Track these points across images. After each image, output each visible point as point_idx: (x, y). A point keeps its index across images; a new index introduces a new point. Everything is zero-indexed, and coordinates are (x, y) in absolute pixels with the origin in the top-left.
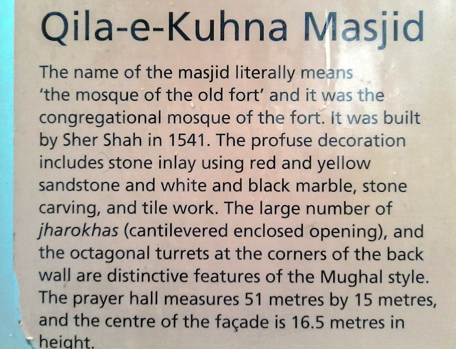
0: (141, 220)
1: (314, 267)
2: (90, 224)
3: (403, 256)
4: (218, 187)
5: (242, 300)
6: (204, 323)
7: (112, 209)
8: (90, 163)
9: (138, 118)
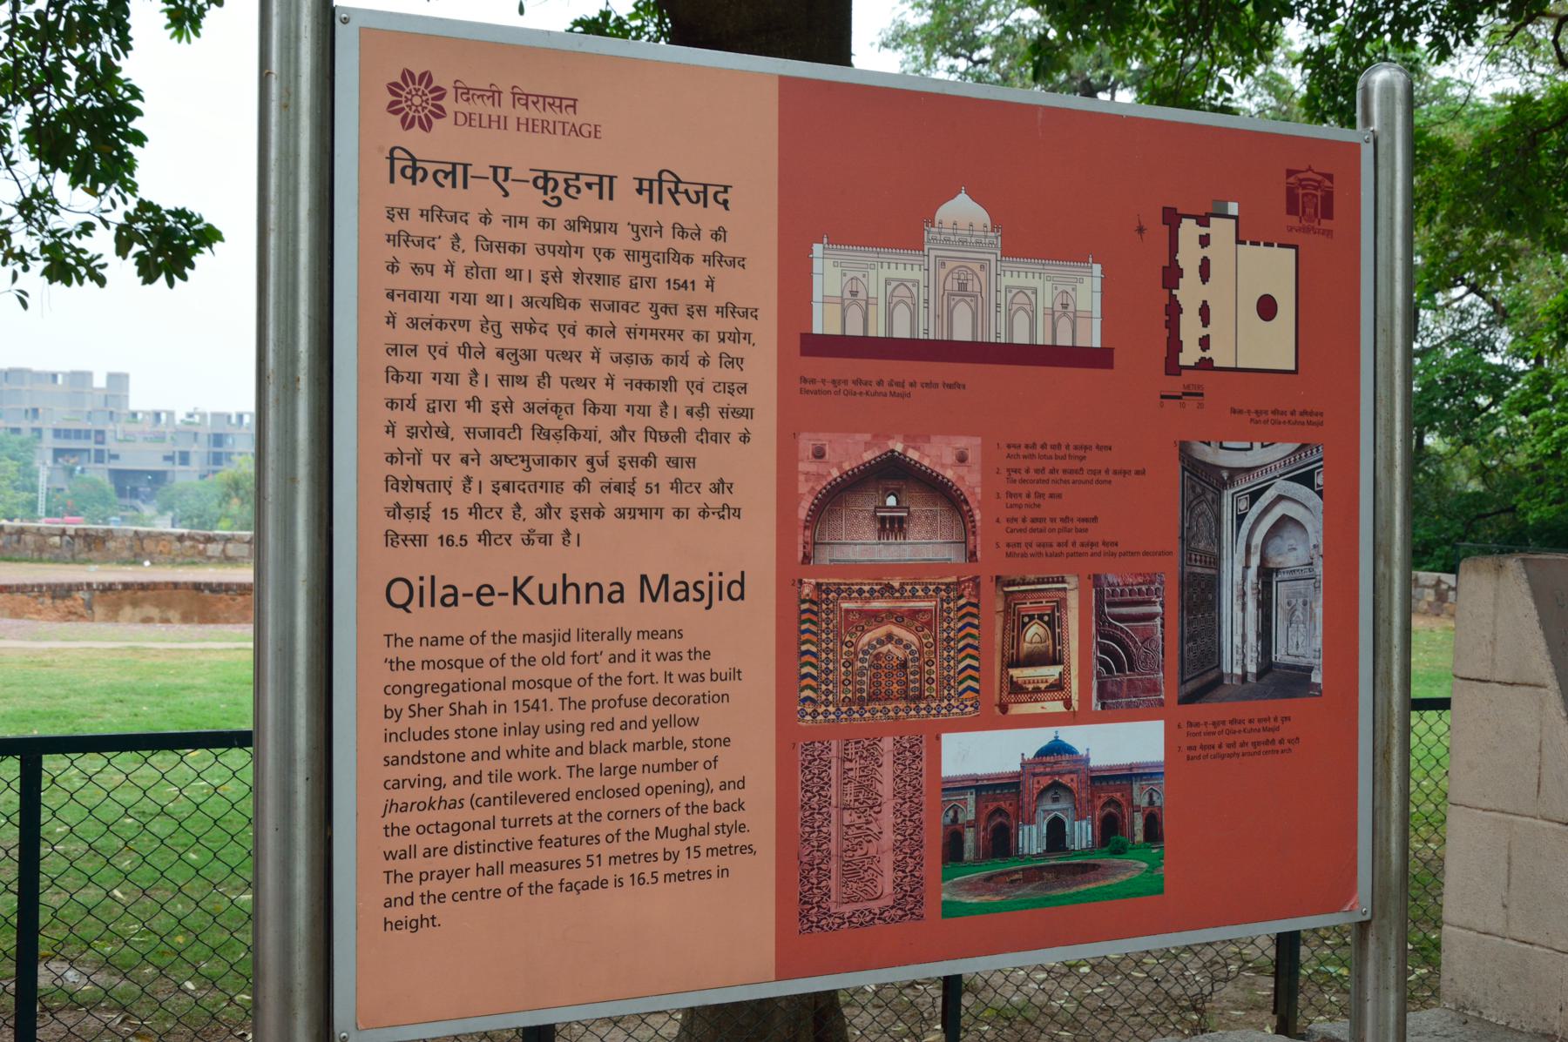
0: (487, 789)
1: (648, 824)
2: (436, 797)
3: (728, 808)
4: (561, 752)
5: (584, 862)
6: (548, 889)
7: (458, 781)
8: (434, 735)
9: (483, 686)
